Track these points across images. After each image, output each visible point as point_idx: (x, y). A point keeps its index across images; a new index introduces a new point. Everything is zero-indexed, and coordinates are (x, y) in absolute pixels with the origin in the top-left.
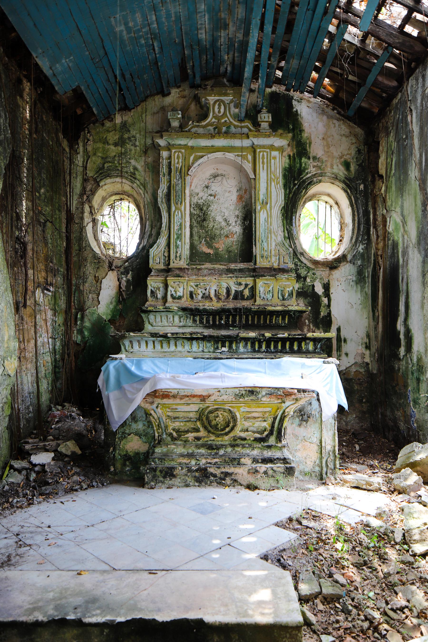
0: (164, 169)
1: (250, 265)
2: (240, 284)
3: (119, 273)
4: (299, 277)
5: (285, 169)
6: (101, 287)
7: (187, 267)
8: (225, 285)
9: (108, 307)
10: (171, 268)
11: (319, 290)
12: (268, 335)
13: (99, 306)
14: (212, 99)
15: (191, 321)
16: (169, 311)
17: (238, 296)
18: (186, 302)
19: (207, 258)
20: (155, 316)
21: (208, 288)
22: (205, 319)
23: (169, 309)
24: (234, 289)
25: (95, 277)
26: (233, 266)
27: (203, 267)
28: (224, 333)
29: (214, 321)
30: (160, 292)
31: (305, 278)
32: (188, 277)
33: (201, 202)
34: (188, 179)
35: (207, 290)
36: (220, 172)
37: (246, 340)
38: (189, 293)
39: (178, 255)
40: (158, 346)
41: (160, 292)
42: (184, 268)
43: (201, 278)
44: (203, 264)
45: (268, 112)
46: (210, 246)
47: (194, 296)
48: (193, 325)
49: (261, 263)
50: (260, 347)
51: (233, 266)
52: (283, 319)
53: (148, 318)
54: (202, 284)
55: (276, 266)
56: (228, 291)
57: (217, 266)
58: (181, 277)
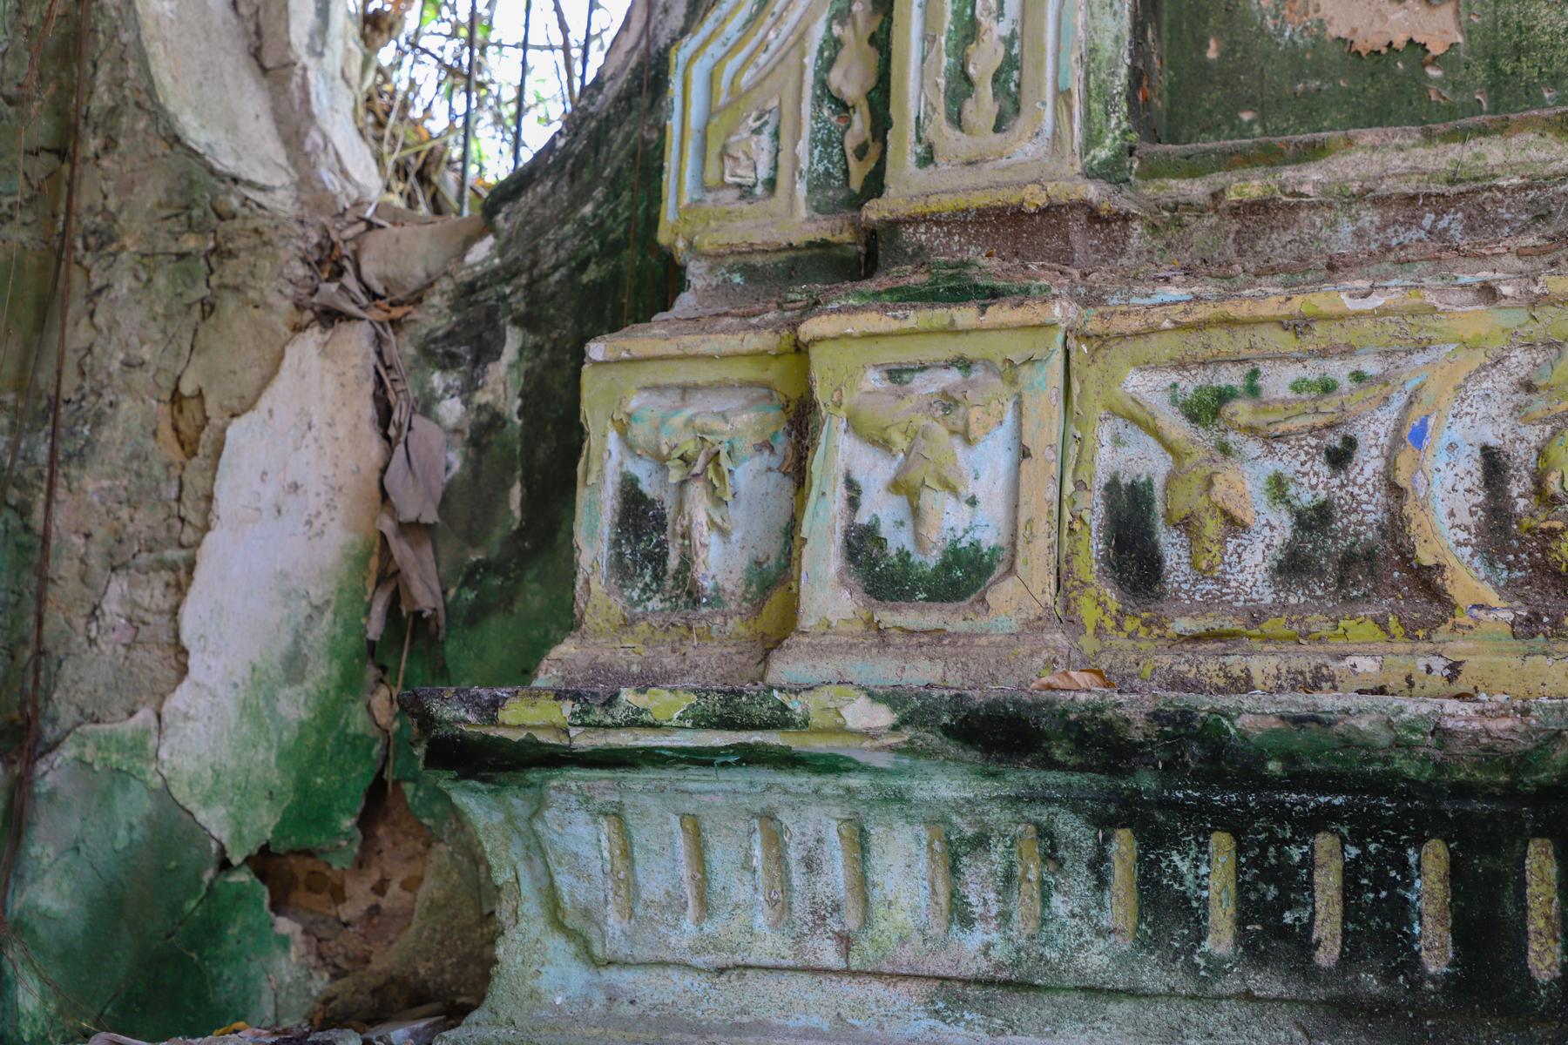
3: (403, 349)
6: (210, 498)
7: (1092, 191)
9: (255, 711)
10: (894, 225)
13: (181, 698)
15: (1120, 908)
16: (789, 761)
20: (617, 815)
21: (1374, 432)
22: (1328, 883)
23: (782, 720)
25: (176, 398)
27: (1311, 178)
30: (737, 516)
32: (1092, 299)
35: (1368, 464)
38: (1094, 509)
39: (984, 61)
41: (737, 516)
42: (1053, 212)
43: (1271, 300)
44: (1313, 152)
47: (1171, 548)
48: (1151, 976)
53: (536, 847)
54: (1278, 381)
58: (995, 294)
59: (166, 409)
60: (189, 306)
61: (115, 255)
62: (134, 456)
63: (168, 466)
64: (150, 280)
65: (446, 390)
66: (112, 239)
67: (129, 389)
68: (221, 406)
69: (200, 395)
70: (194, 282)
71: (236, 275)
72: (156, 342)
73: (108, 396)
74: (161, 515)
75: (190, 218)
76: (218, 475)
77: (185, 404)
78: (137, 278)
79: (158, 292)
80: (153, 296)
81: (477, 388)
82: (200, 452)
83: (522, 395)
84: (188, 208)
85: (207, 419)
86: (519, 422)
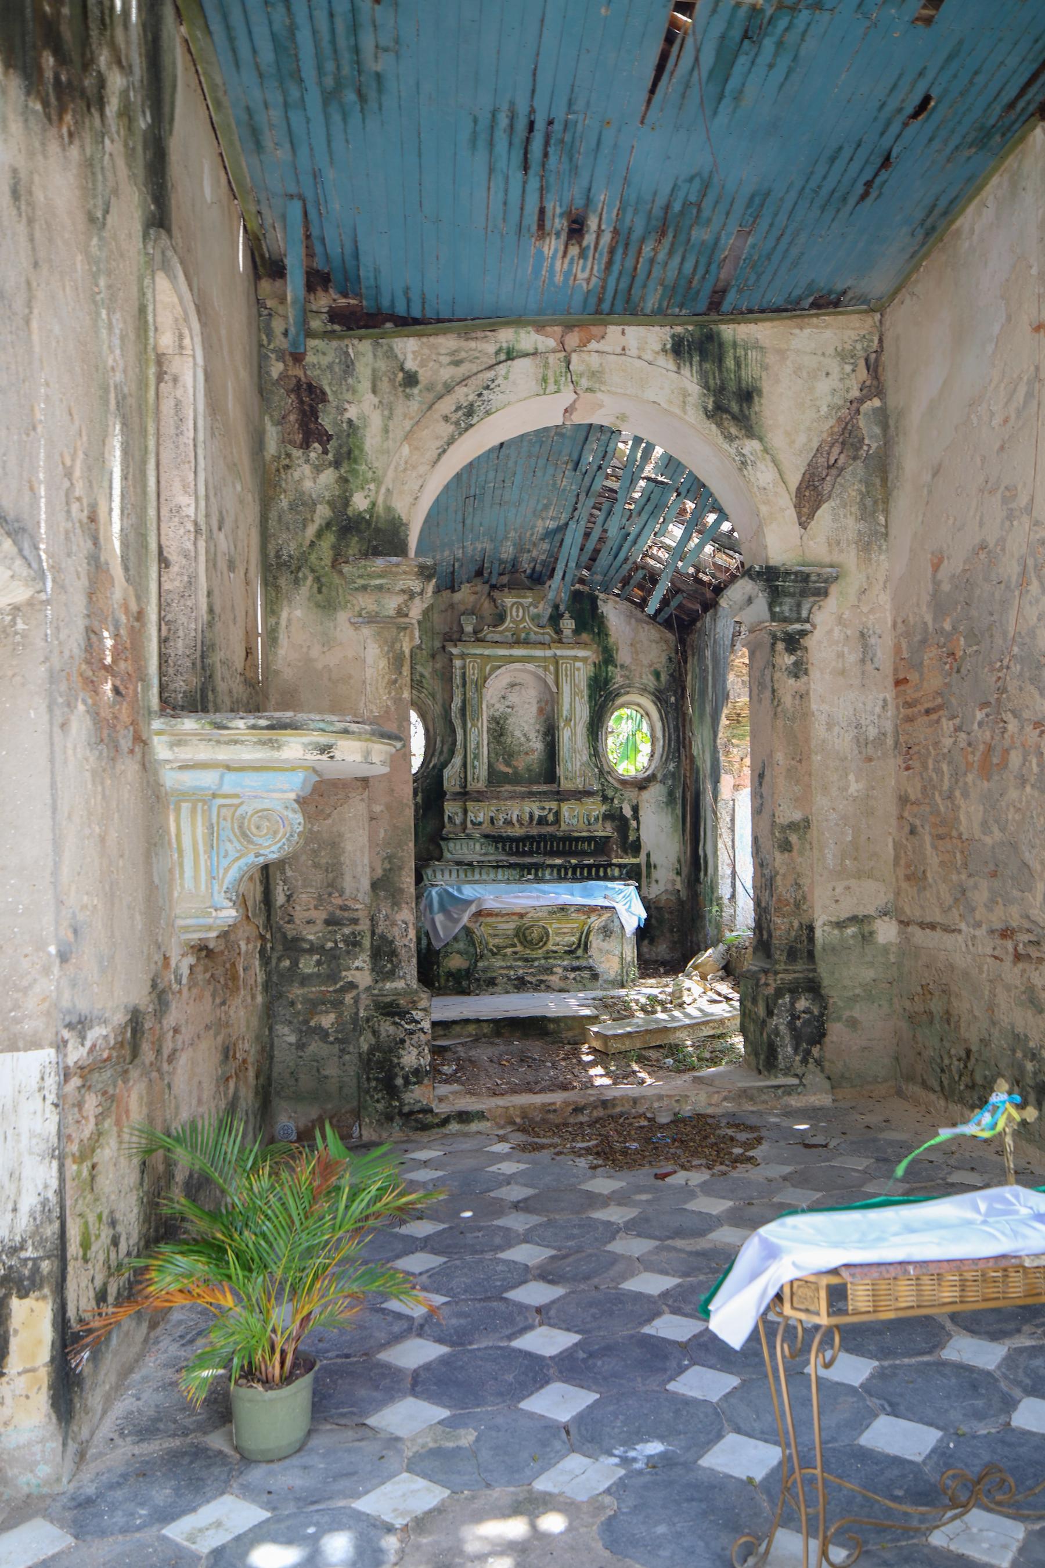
0: (458, 680)
1: (552, 787)
2: (543, 809)
4: (605, 799)
5: (590, 679)
8: (527, 810)
11: (628, 812)
12: (574, 861)
14: (509, 601)
17: (542, 821)
18: (486, 828)
19: (506, 779)
24: (537, 813)
26: (535, 788)
28: (528, 860)
29: (517, 847)
31: (612, 800)
33: (496, 714)
34: (484, 690)
36: (518, 681)
37: (552, 866)
40: (462, 875)
45: (572, 617)
46: (508, 764)
49: (565, 785)
50: (566, 874)
51: (535, 788)
52: (589, 845)
55: (581, 787)
56: (531, 815)
57: (518, 789)
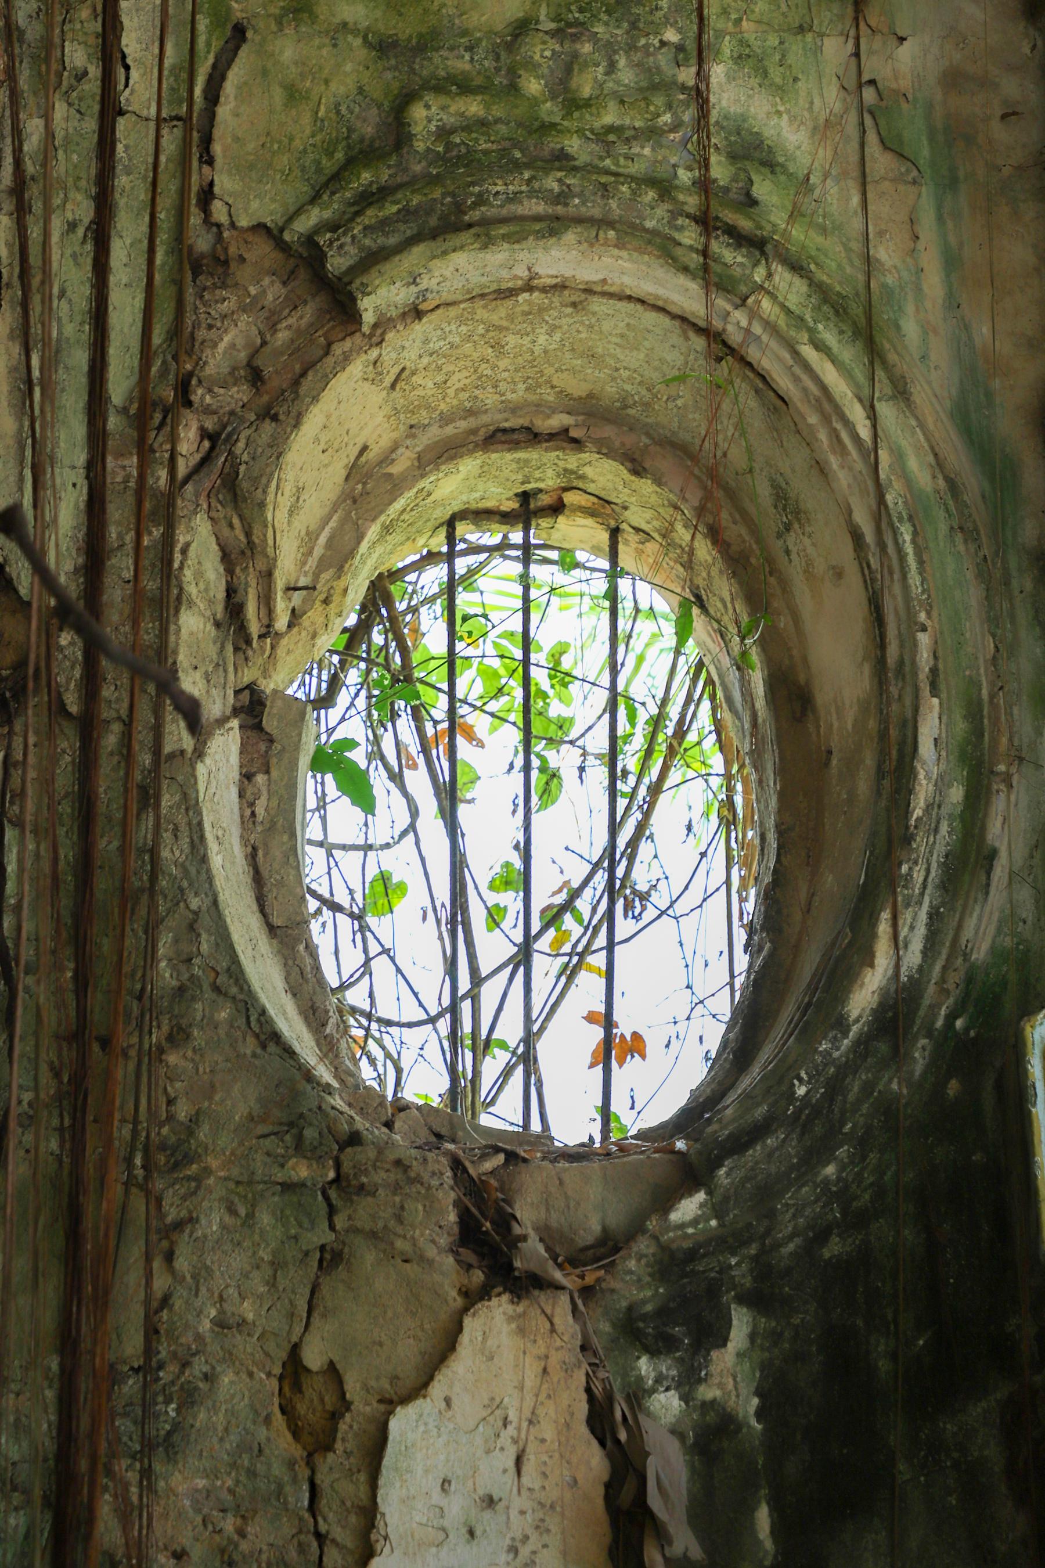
59: (275, 1384)
60: (307, 1254)
61: (198, 1179)
62: (242, 1447)
63: (291, 1464)
64: (251, 1215)
65: (658, 1380)
66: (189, 1159)
67: (229, 1357)
68: (367, 1389)
69: (332, 1370)
70: (313, 1222)
71: (374, 1217)
72: (260, 1297)
73: (199, 1366)
74: (287, 1529)
75: (299, 1138)
76: (381, 1482)
77: (306, 1381)
78: (232, 1211)
79: (262, 1232)
80: (257, 1237)
81: (700, 1381)
82: (339, 1446)
83: (758, 1393)
84: (291, 1124)
85: (347, 1405)
86: (759, 1427)
